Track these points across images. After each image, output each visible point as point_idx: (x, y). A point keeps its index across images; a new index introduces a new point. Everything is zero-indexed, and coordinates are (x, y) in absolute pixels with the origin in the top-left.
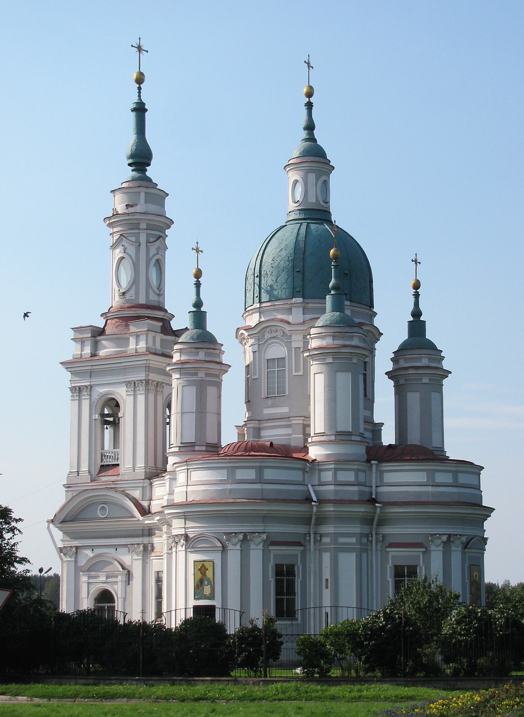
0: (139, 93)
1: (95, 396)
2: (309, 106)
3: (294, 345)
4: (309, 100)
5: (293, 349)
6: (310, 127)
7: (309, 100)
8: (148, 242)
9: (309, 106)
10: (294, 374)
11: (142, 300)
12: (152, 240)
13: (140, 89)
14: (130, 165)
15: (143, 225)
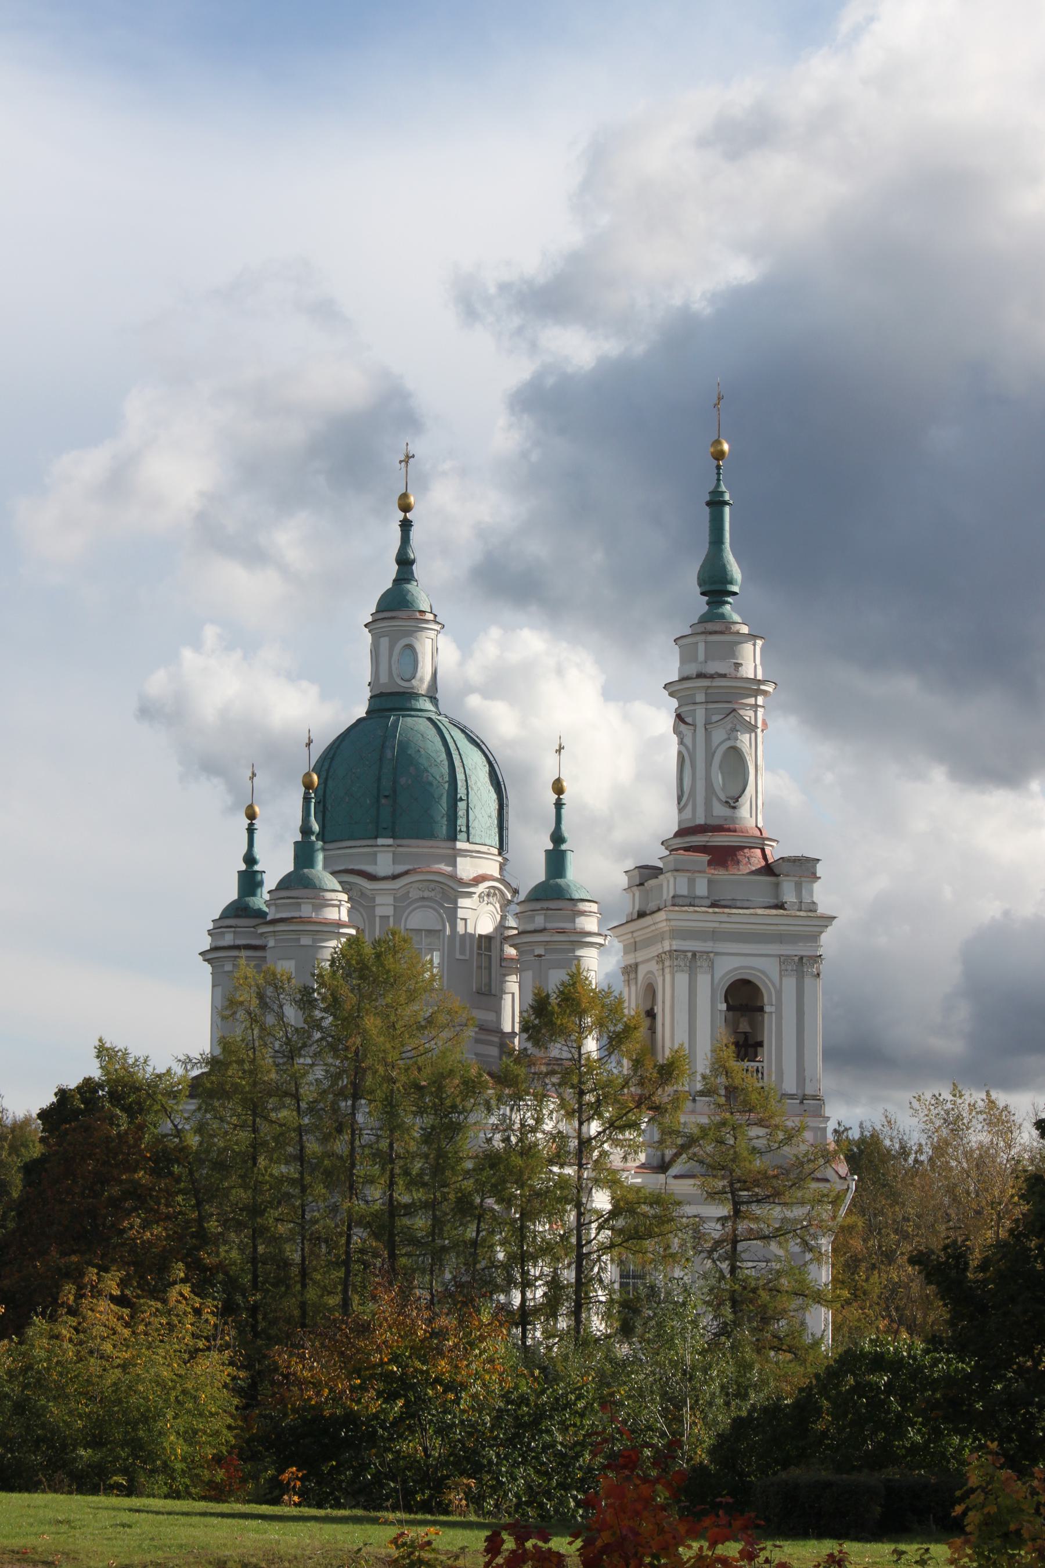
0: (719, 474)
1: (718, 975)
2: (406, 526)
3: (380, 911)
4: (405, 516)
5: (377, 919)
6: (405, 562)
7: (405, 516)
8: (707, 723)
9: (406, 526)
10: (458, 956)
11: (701, 820)
12: (715, 718)
13: (718, 467)
14: (703, 594)
15: (700, 697)
